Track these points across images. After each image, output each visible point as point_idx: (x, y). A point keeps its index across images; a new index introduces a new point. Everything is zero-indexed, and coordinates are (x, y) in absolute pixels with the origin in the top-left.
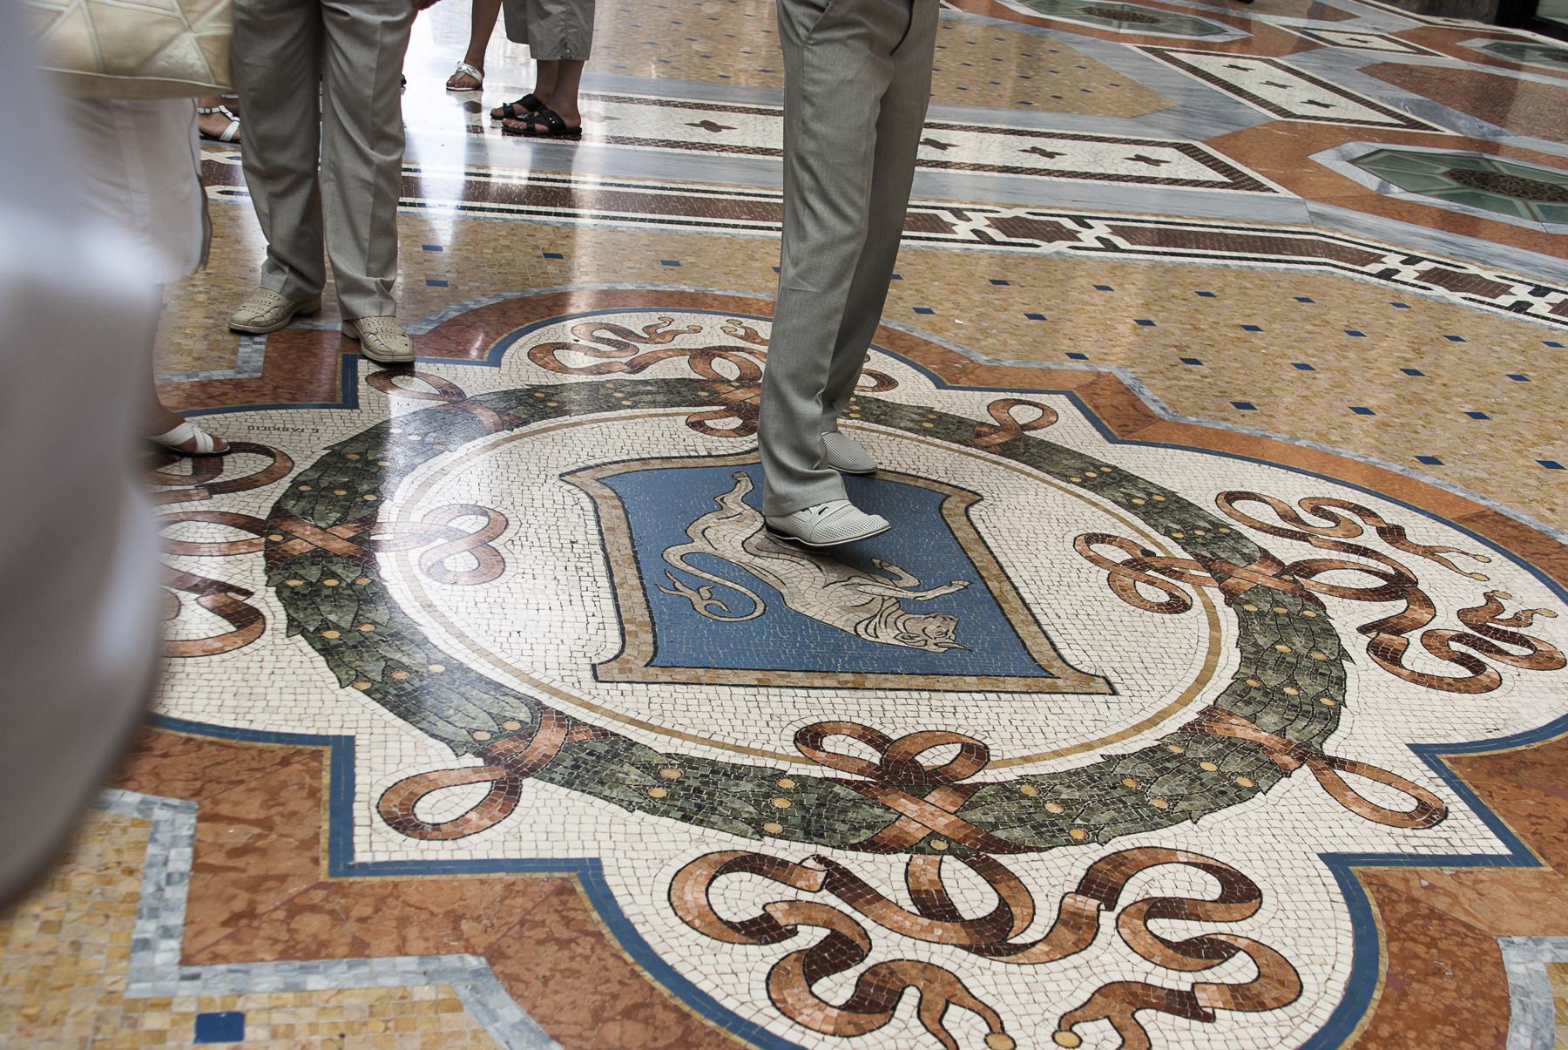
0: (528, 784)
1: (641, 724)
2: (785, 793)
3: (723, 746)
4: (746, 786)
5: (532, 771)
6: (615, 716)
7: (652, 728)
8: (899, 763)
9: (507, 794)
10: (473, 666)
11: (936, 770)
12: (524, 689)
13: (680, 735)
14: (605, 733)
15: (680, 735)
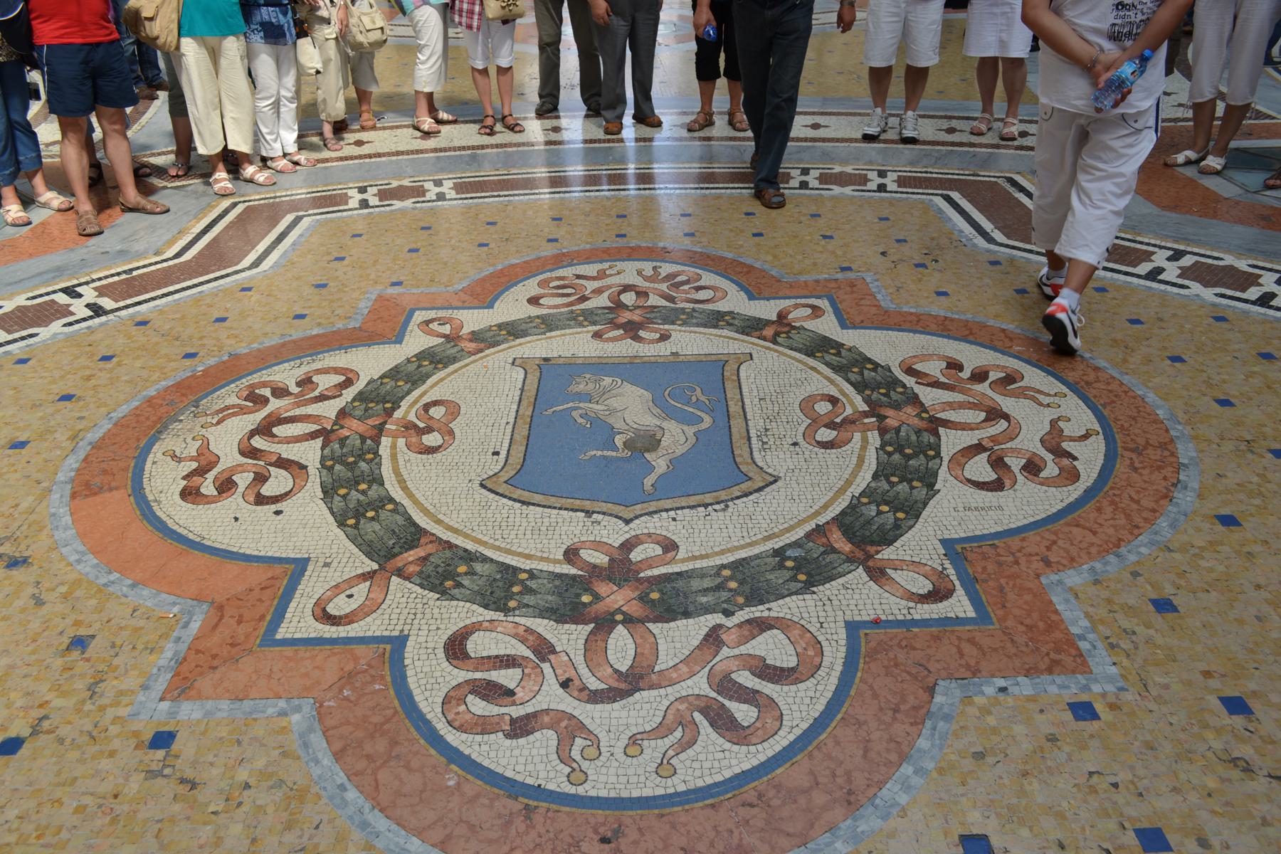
0: (775, 319)
1: (732, 338)
2: (681, 320)
3: (700, 333)
4: (694, 321)
5: (773, 322)
6: (742, 341)
7: (728, 337)
8: (631, 330)
9: (782, 316)
10: (803, 356)
11: (618, 328)
12: (781, 349)
13: (717, 336)
14: (747, 335)
15: (717, 336)
